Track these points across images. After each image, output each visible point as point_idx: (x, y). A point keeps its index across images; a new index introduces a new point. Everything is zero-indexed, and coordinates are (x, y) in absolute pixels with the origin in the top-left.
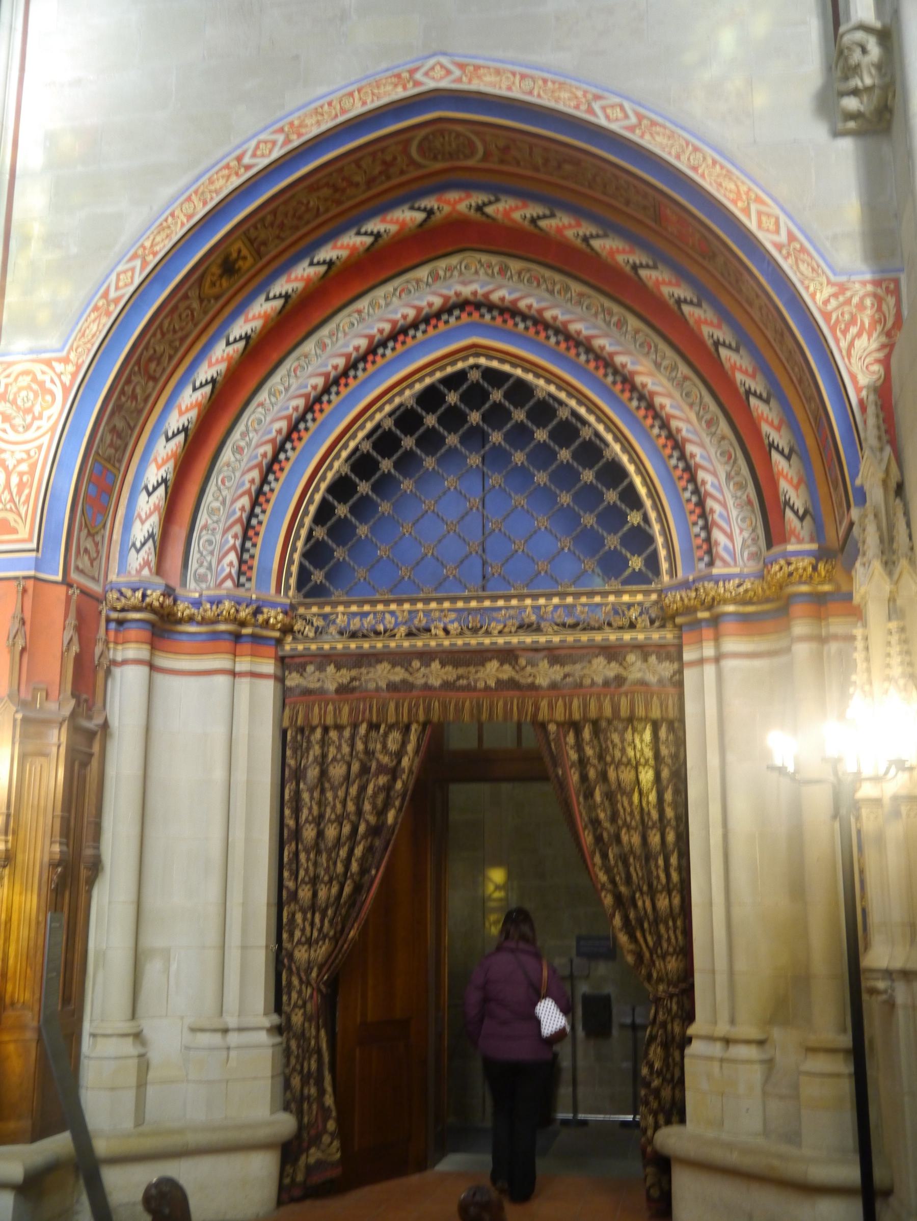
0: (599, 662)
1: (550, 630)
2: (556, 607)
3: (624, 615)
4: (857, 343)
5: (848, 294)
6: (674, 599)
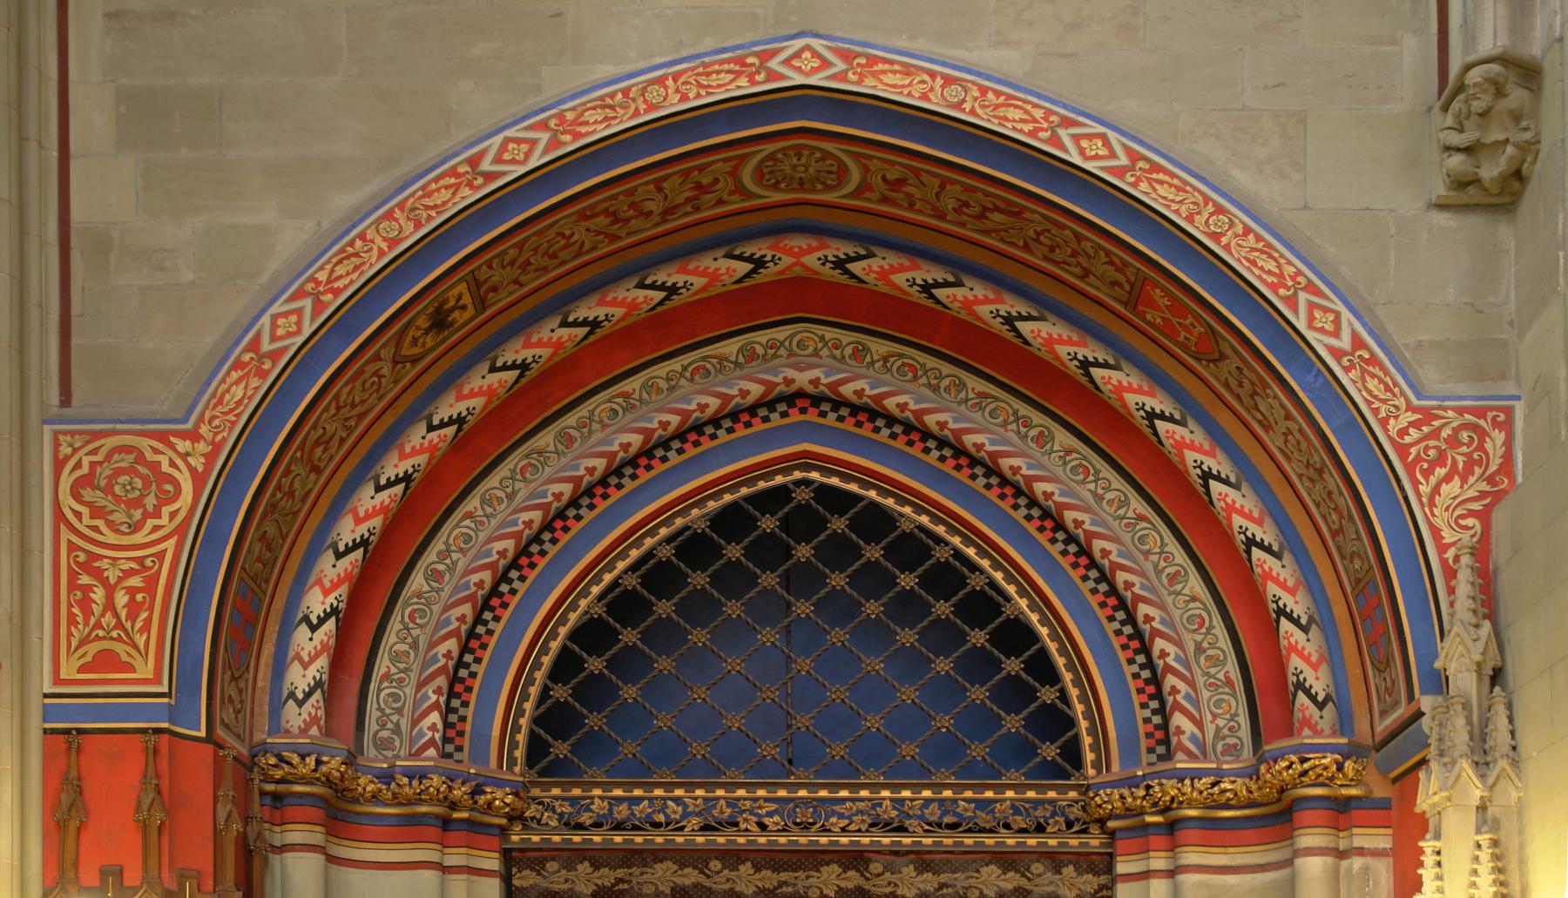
0: (991, 872)
1: (918, 830)
2: (928, 801)
3: (1028, 815)
4: (1445, 488)
5: (1436, 423)
6: (1109, 799)
